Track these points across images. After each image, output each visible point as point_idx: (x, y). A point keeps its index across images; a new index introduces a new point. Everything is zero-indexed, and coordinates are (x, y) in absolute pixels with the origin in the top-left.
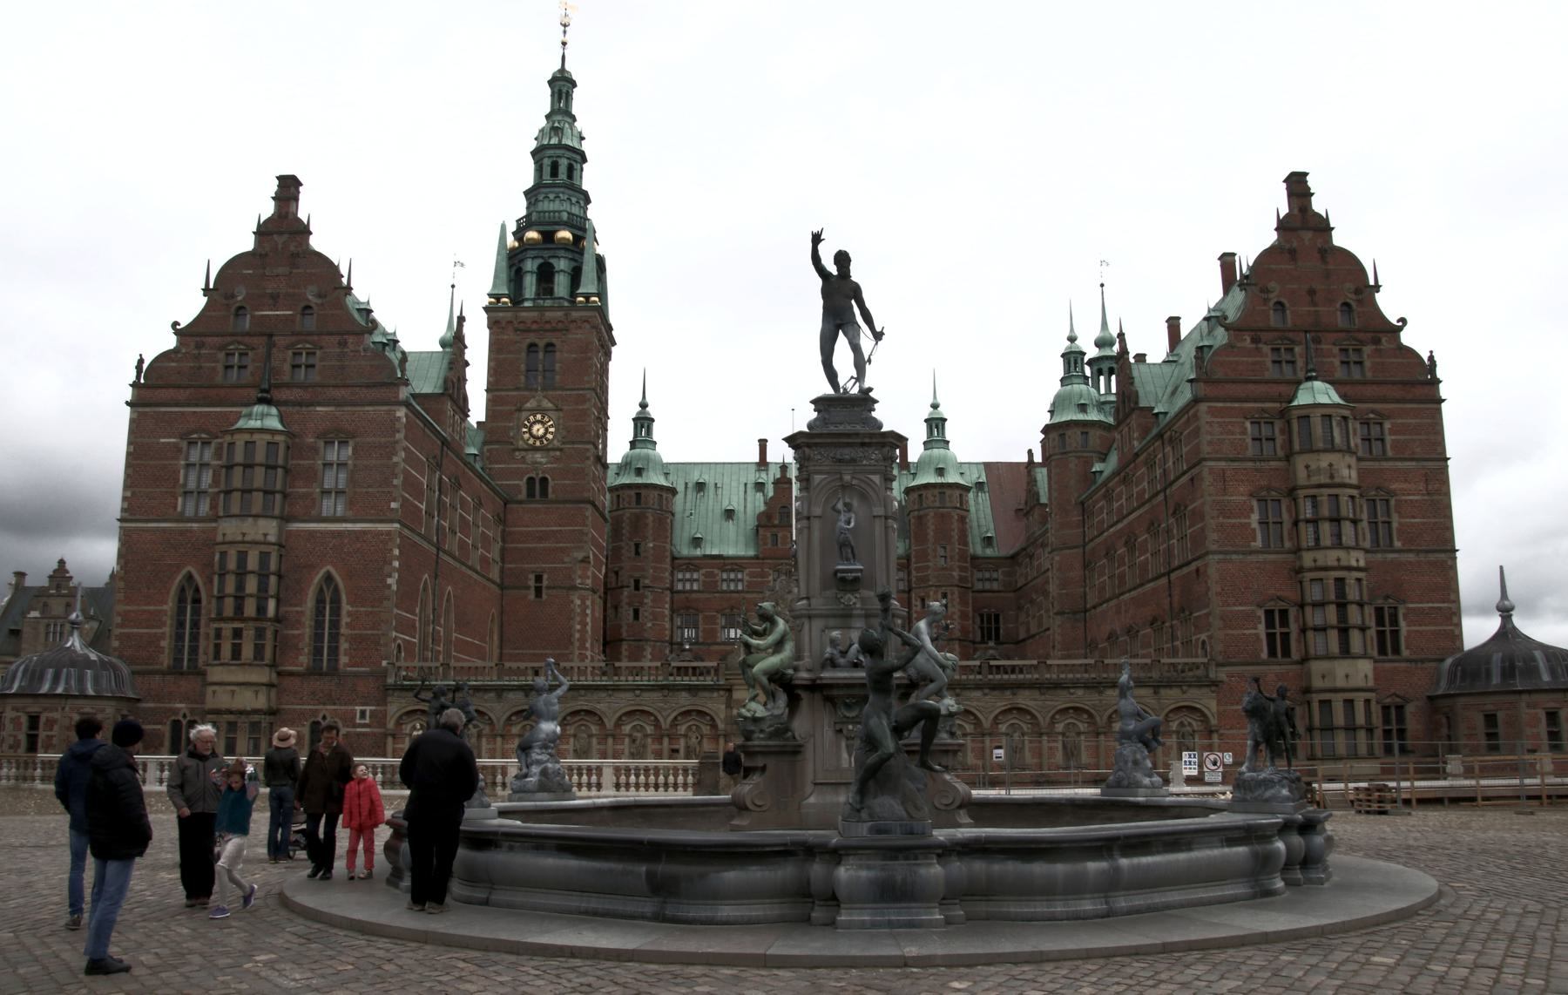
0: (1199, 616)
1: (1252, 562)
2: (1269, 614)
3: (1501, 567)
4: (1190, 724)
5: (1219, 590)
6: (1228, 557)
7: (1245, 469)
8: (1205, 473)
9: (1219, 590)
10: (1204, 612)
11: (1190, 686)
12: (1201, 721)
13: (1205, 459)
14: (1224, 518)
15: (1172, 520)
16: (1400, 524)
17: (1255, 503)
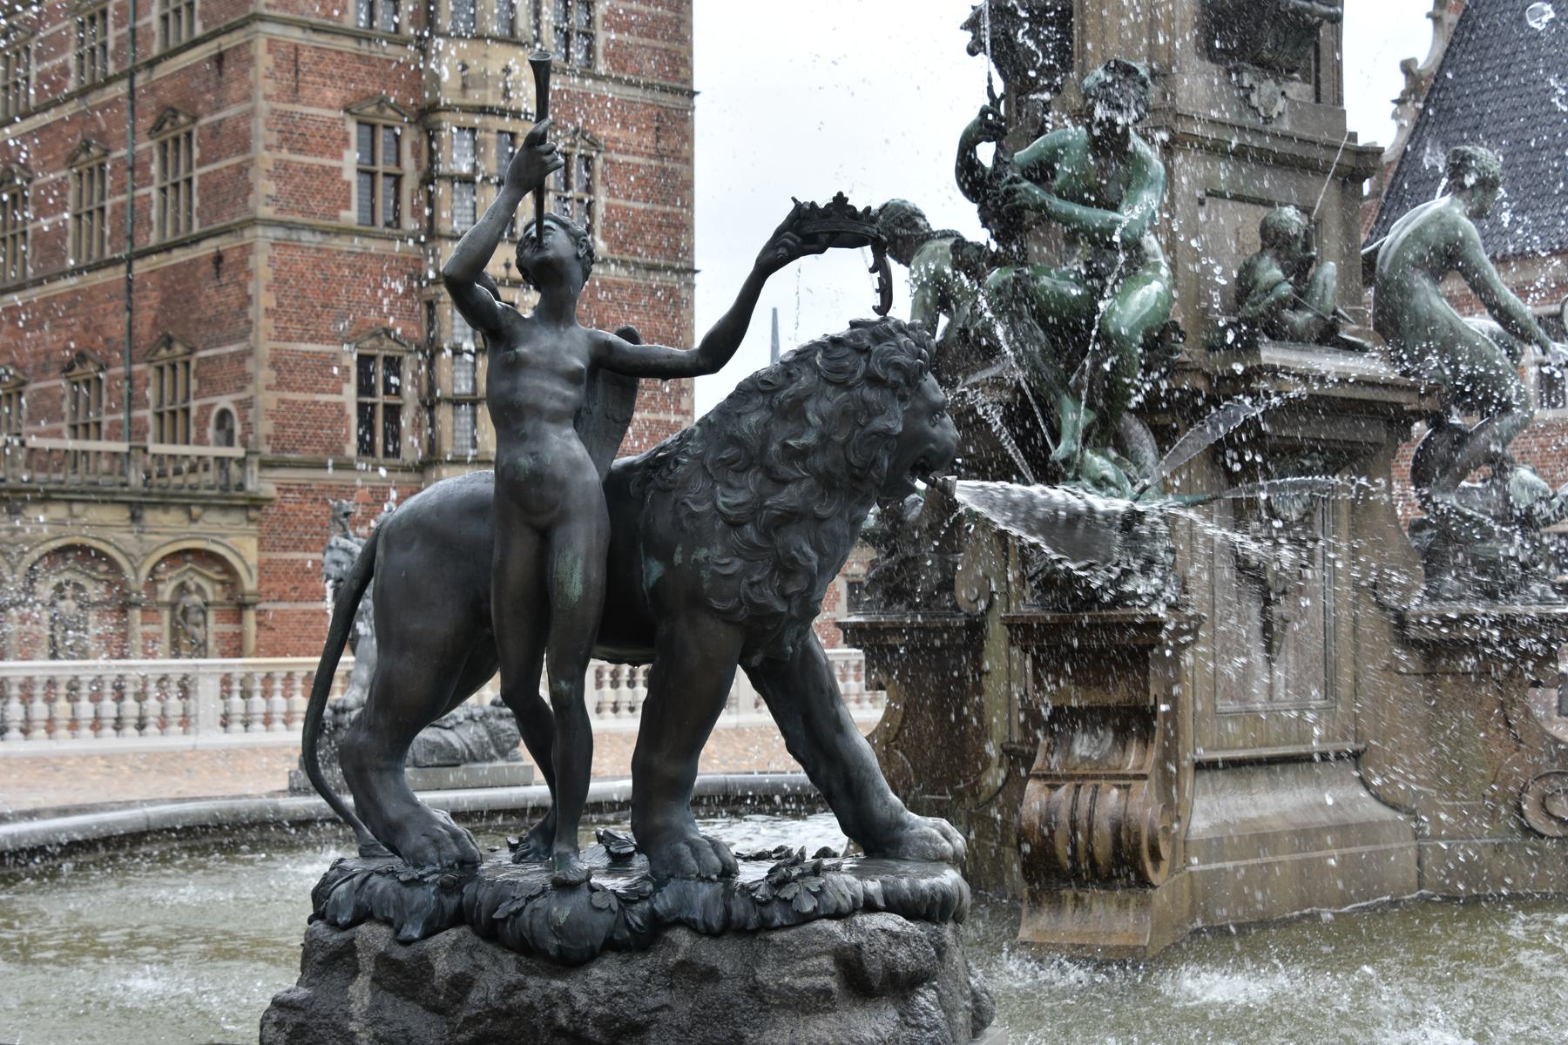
0: (219, 357)
1: (340, 253)
2: (365, 361)
3: (775, 311)
4: (200, 589)
5: (273, 304)
6: (294, 236)
7: (339, 53)
8: (260, 49)
9: (273, 304)
10: (232, 348)
11: (206, 507)
12: (222, 583)
13: (262, 18)
14: (291, 150)
15: (146, 145)
16: (608, 208)
17: (352, 127)
